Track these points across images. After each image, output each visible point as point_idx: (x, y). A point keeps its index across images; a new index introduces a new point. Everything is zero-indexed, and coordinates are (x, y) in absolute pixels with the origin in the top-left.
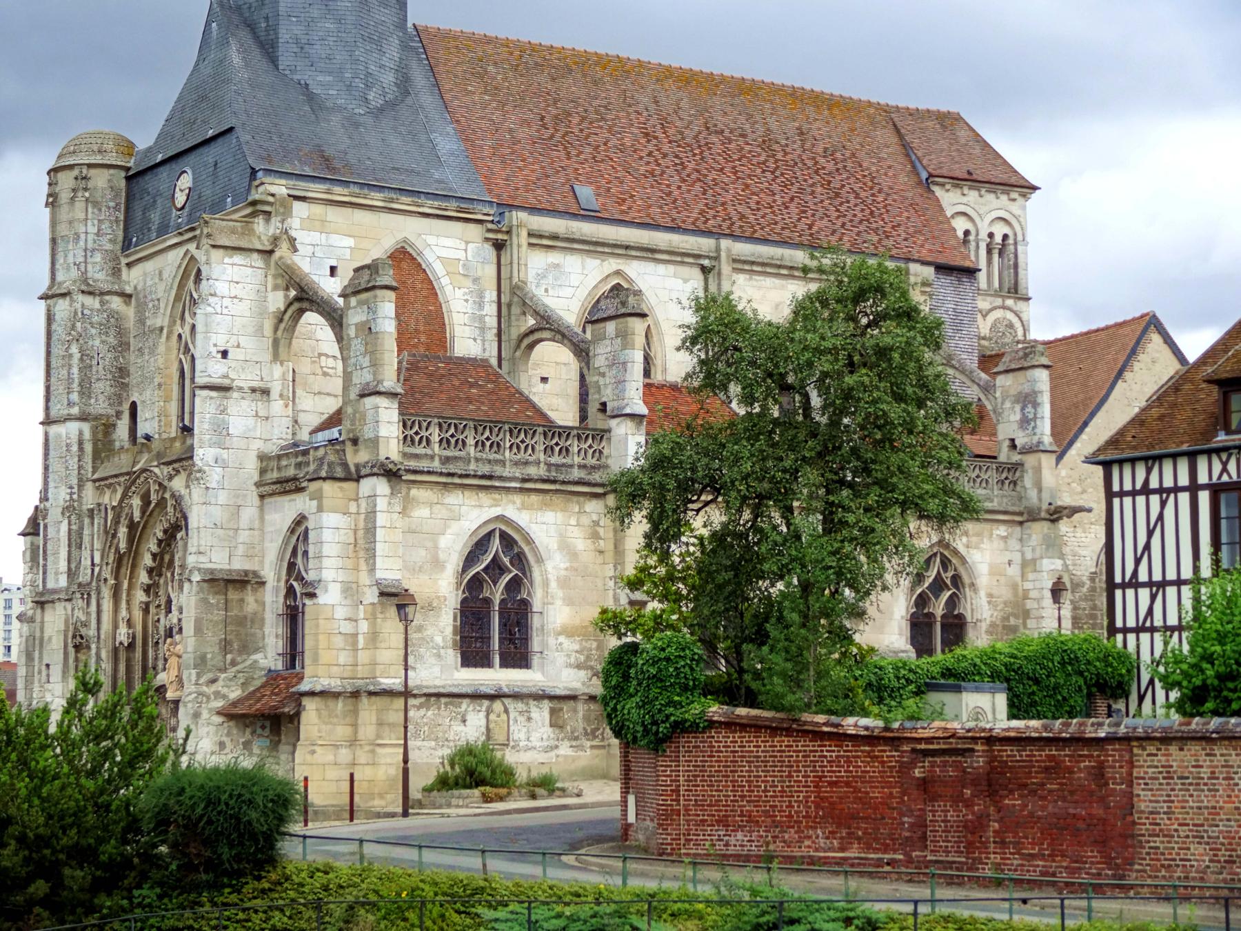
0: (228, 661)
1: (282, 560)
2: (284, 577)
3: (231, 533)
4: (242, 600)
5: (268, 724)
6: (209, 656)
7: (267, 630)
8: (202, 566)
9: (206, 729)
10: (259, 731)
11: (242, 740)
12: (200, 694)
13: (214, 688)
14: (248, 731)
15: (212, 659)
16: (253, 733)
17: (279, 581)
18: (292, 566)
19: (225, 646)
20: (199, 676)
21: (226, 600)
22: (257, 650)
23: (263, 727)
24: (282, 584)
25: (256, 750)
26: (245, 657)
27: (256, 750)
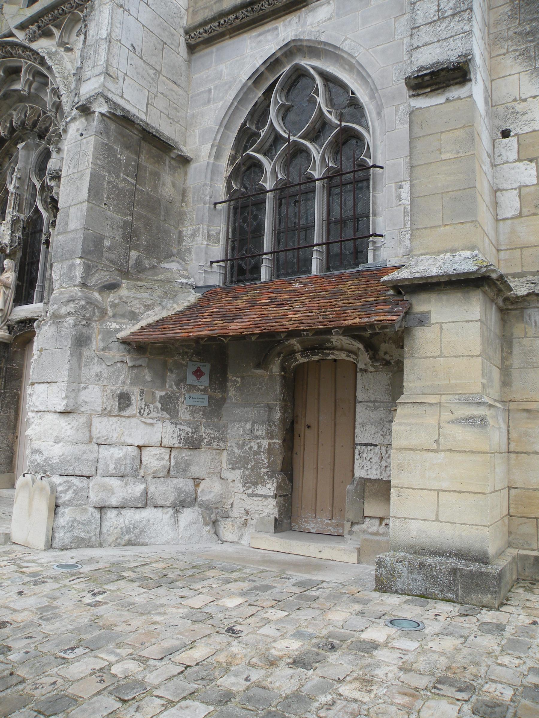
0: (132, 262)
1: (227, 127)
2: (228, 151)
3: (152, 72)
4: (156, 175)
5: (206, 368)
6: (107, 243)
7: (187, 230)
8: (110, 96)
9: (96, 368)
10: (191, 379)
11: (159, 394)
12: (90, 302)
13: (112, 297)
14: (171, 377)
15: (110, 249)
16: (181, 380)
17: (217, 157)
18: (246, 138)
19: (130, 236)
20: (88, 270)
21: (138, 167)
22: (169, 256)
23: (198, 373)
24: (224, 161)
25: (184, 415)
26: (154, 261)
27: (184, 415)
